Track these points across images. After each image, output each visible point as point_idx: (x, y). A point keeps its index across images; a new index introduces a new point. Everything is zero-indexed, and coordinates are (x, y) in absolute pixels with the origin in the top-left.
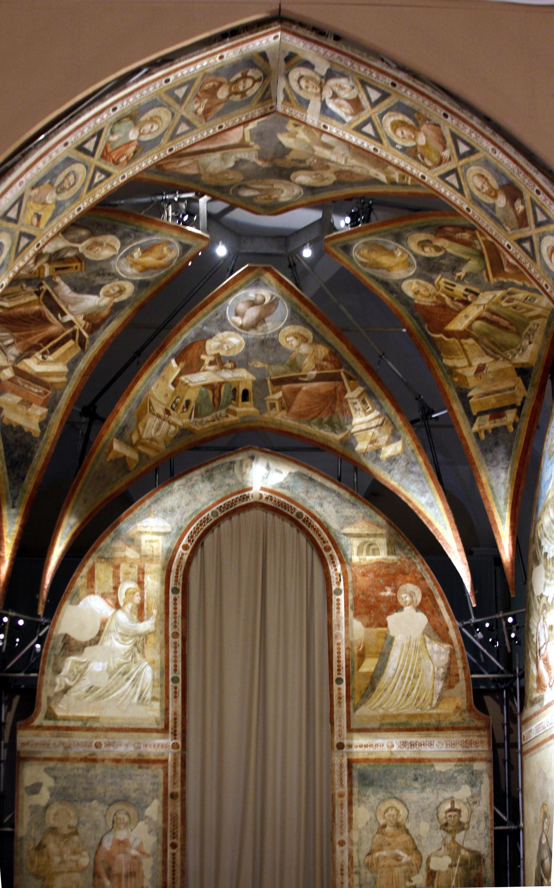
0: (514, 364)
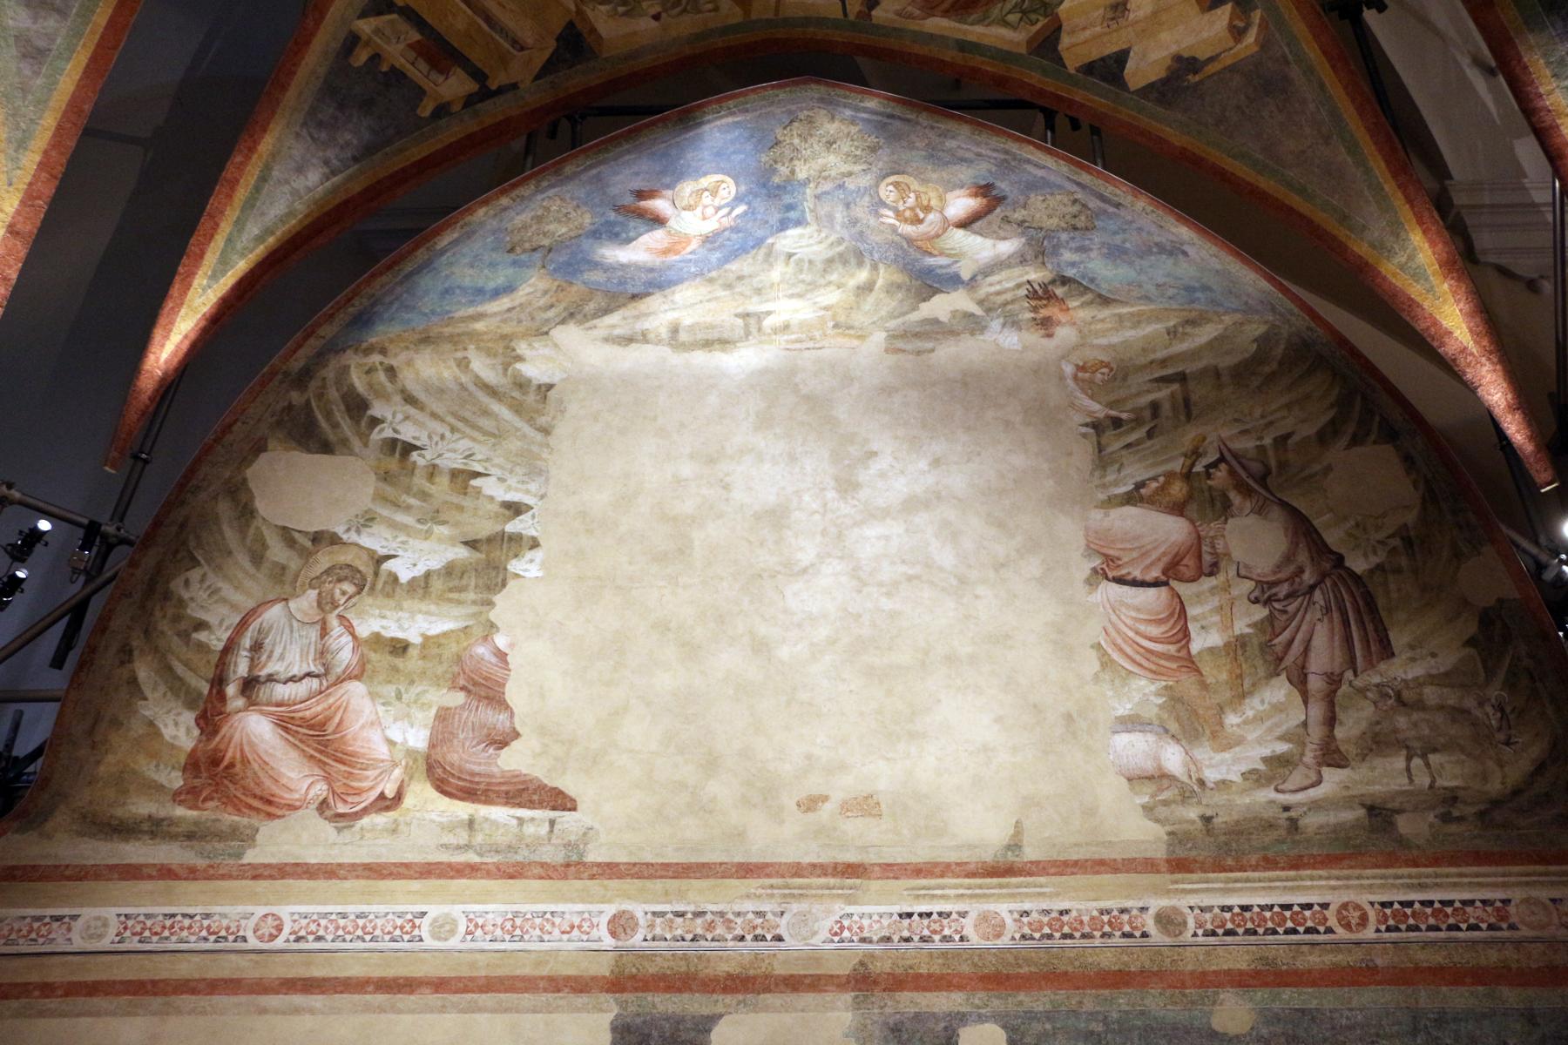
0: (579, 12)
